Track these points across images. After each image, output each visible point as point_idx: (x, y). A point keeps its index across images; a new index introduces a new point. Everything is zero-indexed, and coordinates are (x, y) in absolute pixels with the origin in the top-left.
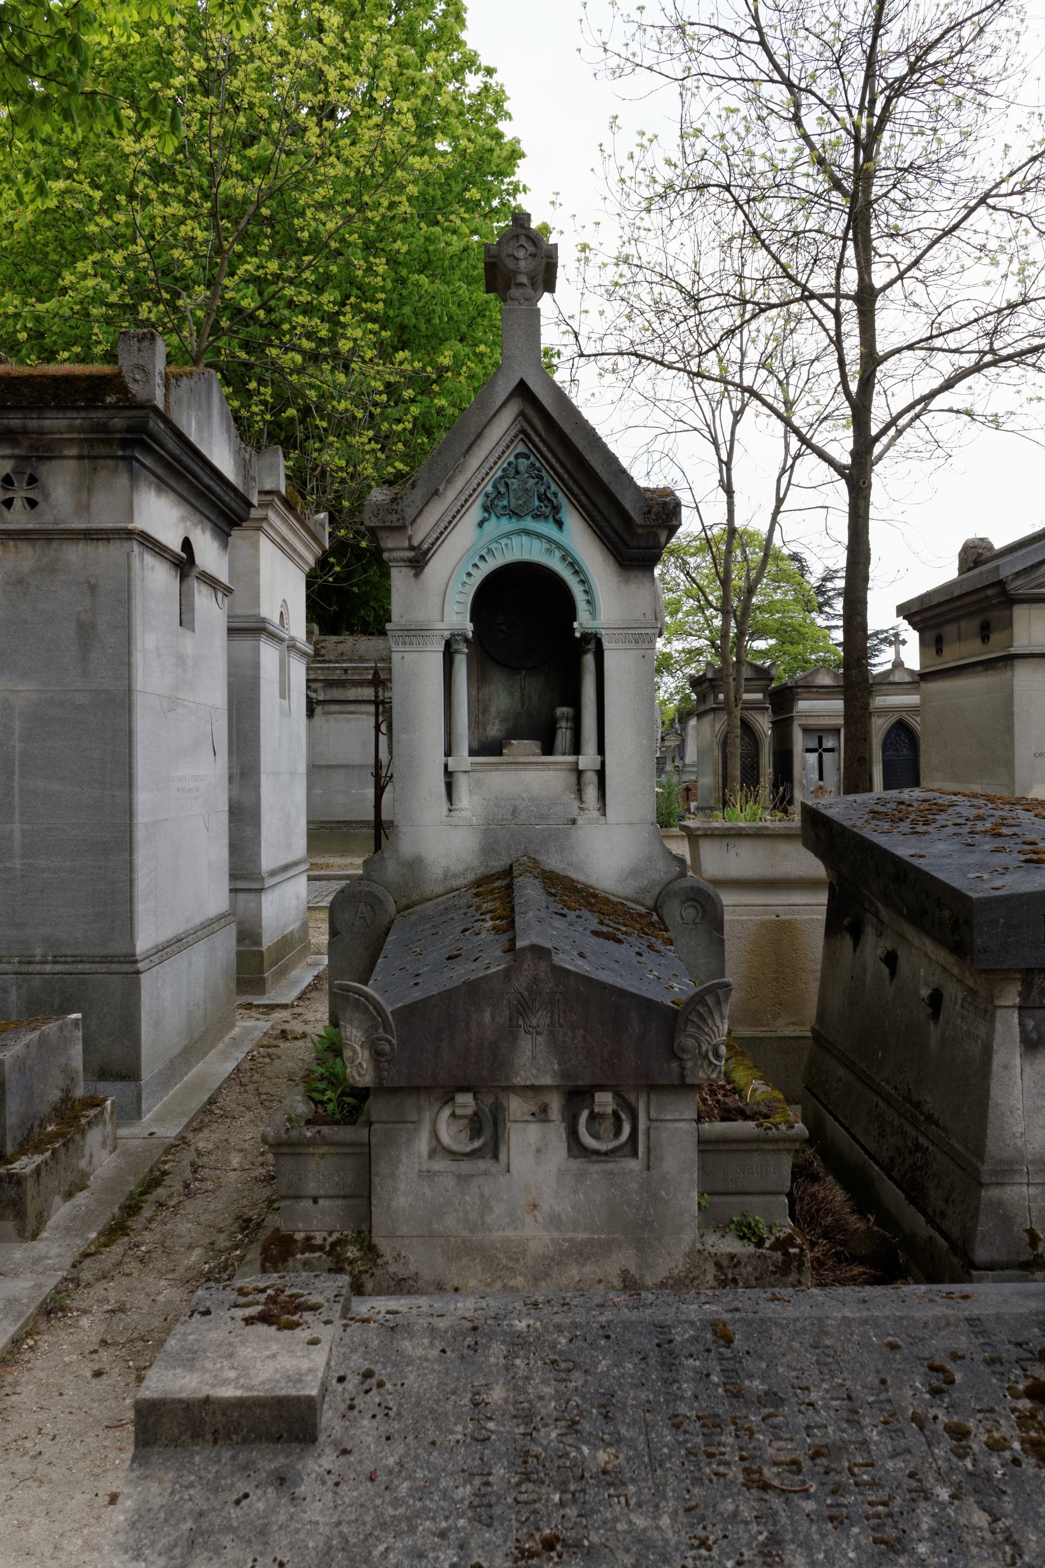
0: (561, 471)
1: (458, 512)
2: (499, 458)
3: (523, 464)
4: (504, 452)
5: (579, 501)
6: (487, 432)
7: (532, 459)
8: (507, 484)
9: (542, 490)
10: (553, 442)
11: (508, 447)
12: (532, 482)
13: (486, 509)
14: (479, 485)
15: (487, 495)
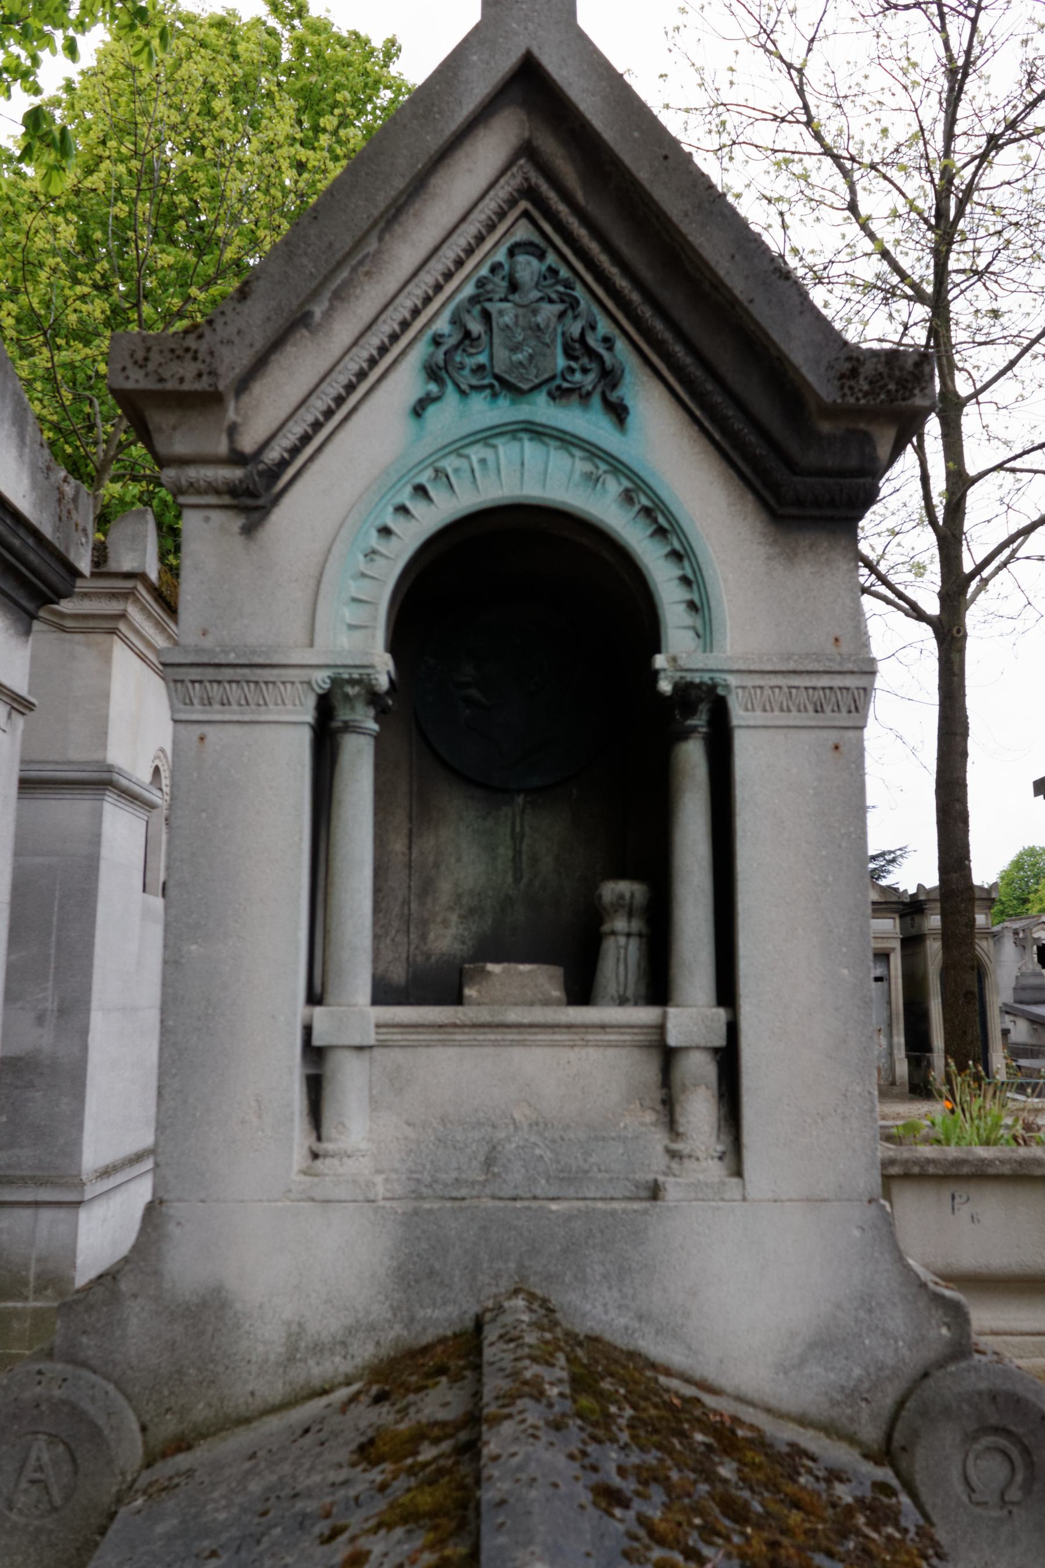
0: (622, 283)
1: (362, 375)
2: (470, 251)
3: (528, 268)
4: (480, 239)
5: (667, 357)
6: (438, 181)
7: (551, 258)
8: (487, 317)
9: (575, 329)
10: (604, 215)
11: (492, 227)
12: (548, 312)
13: (433, 372)
14: (416, 312)
15: (437, 341)
